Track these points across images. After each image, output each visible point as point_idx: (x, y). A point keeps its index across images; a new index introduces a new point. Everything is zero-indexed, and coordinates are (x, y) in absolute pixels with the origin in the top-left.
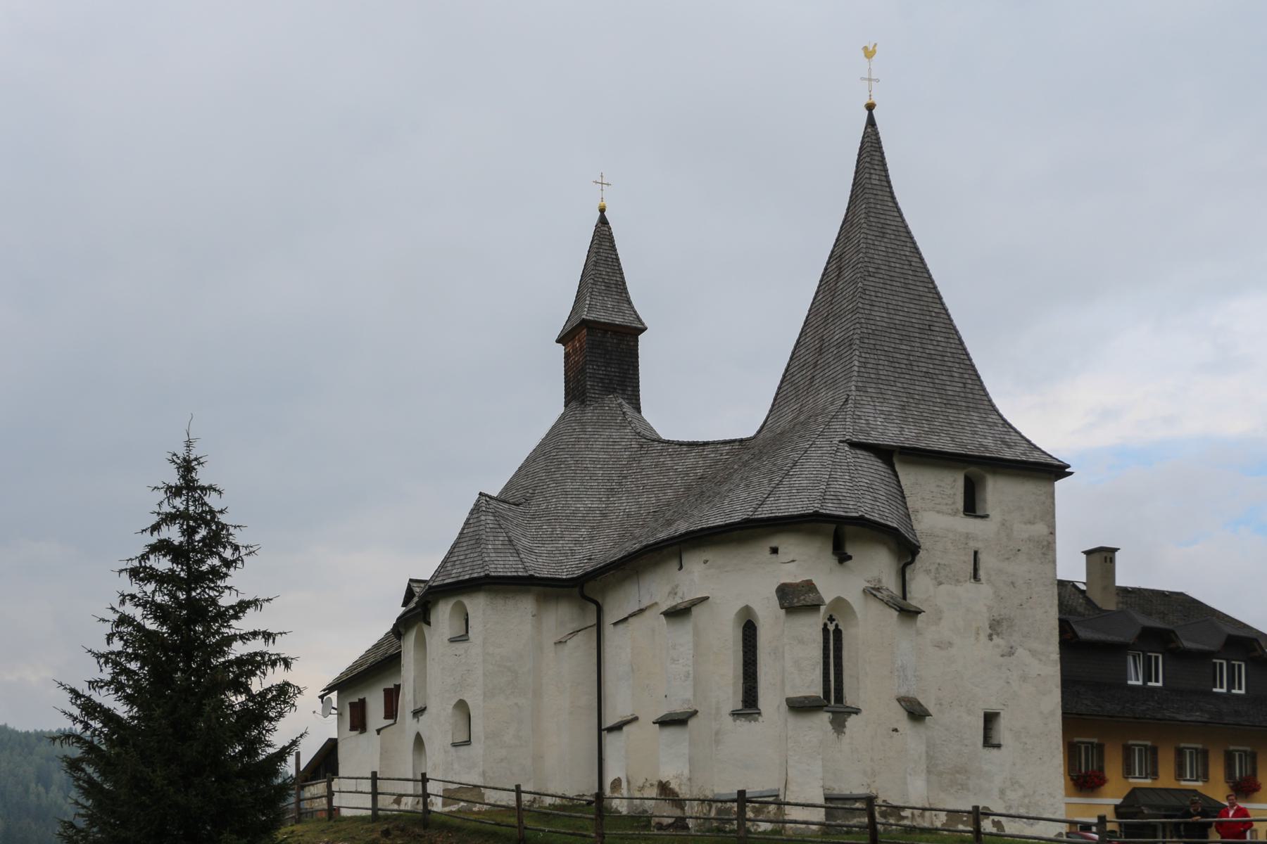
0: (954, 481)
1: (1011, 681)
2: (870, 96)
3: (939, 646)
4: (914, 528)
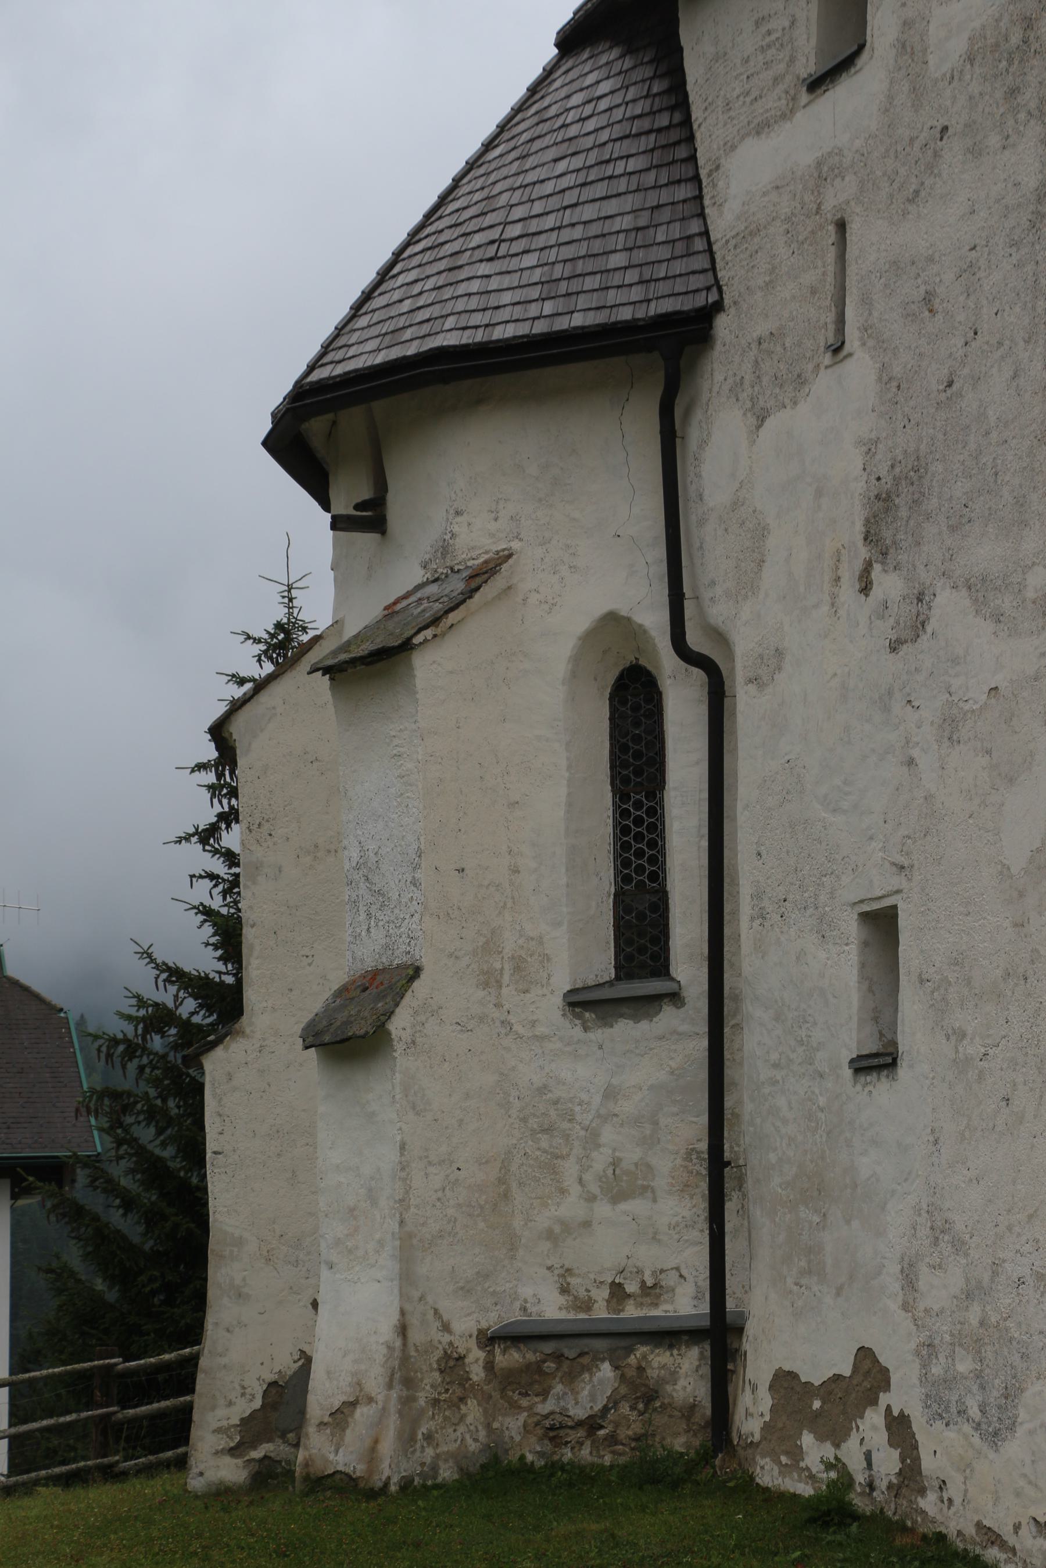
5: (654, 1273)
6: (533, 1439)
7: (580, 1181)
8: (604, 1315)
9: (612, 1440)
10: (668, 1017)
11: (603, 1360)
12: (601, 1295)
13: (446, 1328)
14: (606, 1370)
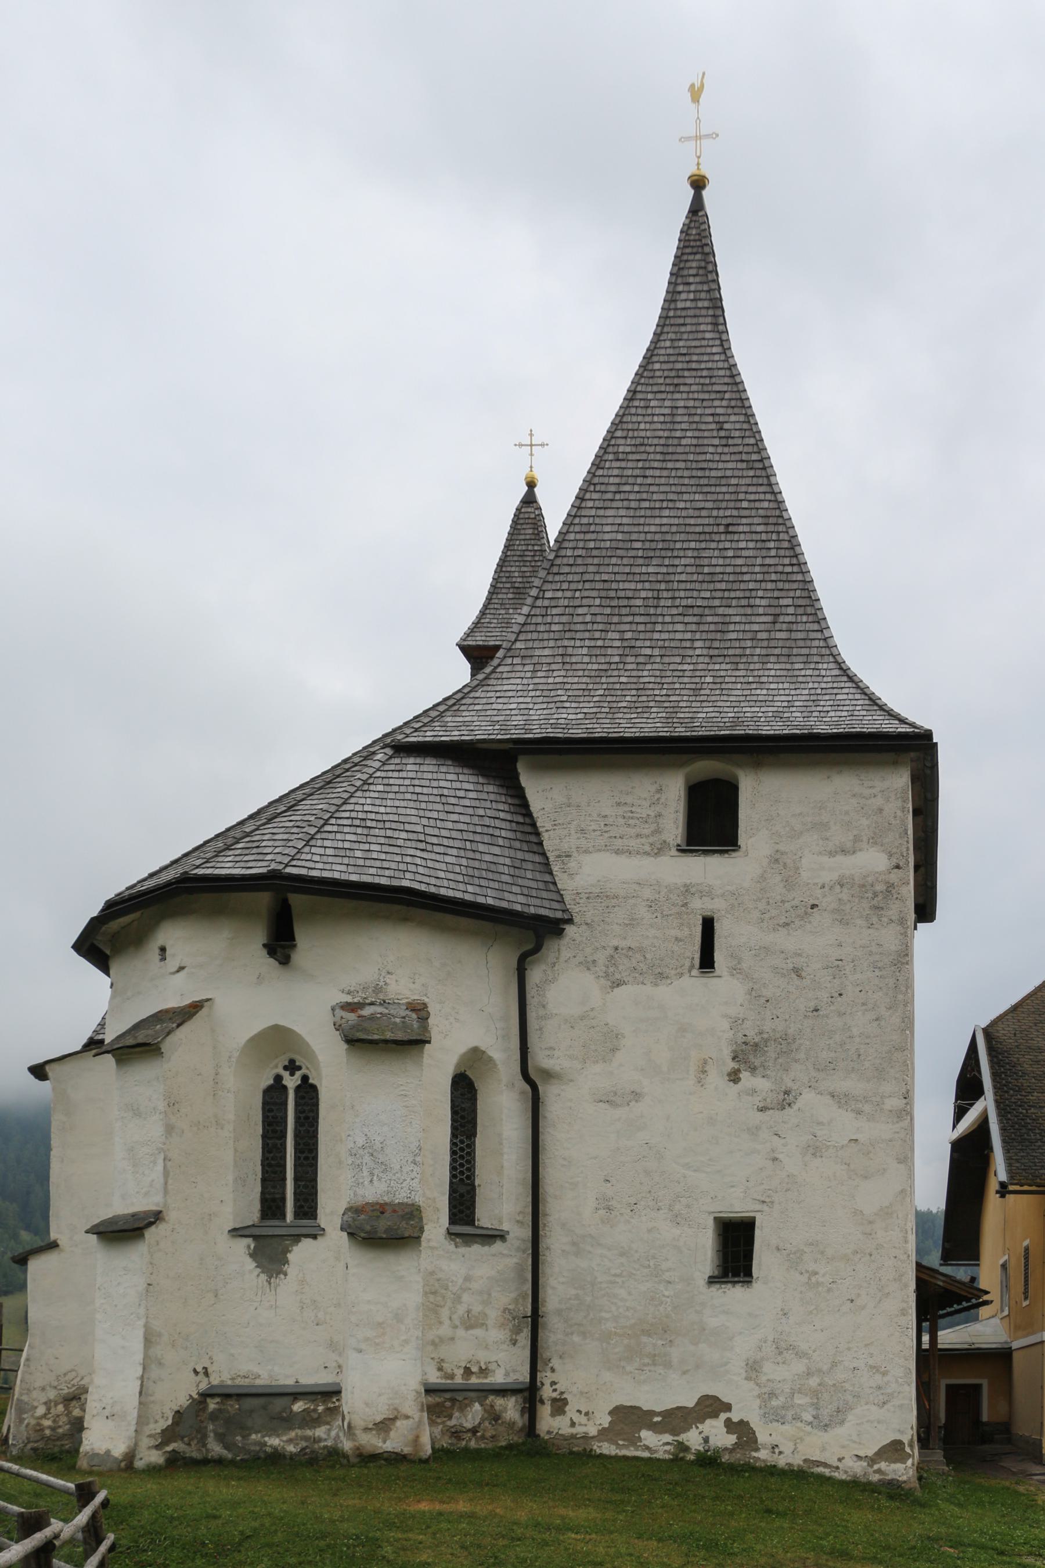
0: (660, 791)
1: (780, 1156)
2: (698, 164)
3: (609, 1100)
4: (559, 886)
5: (485, 1363)
6: (446, 1438)
7: (450, 1318)
8: (461, 1381)
9: (483, 1437)
10: (498, 1246)
11: (475, 1402)
12: (459, 1372)
14: (477, 1406)
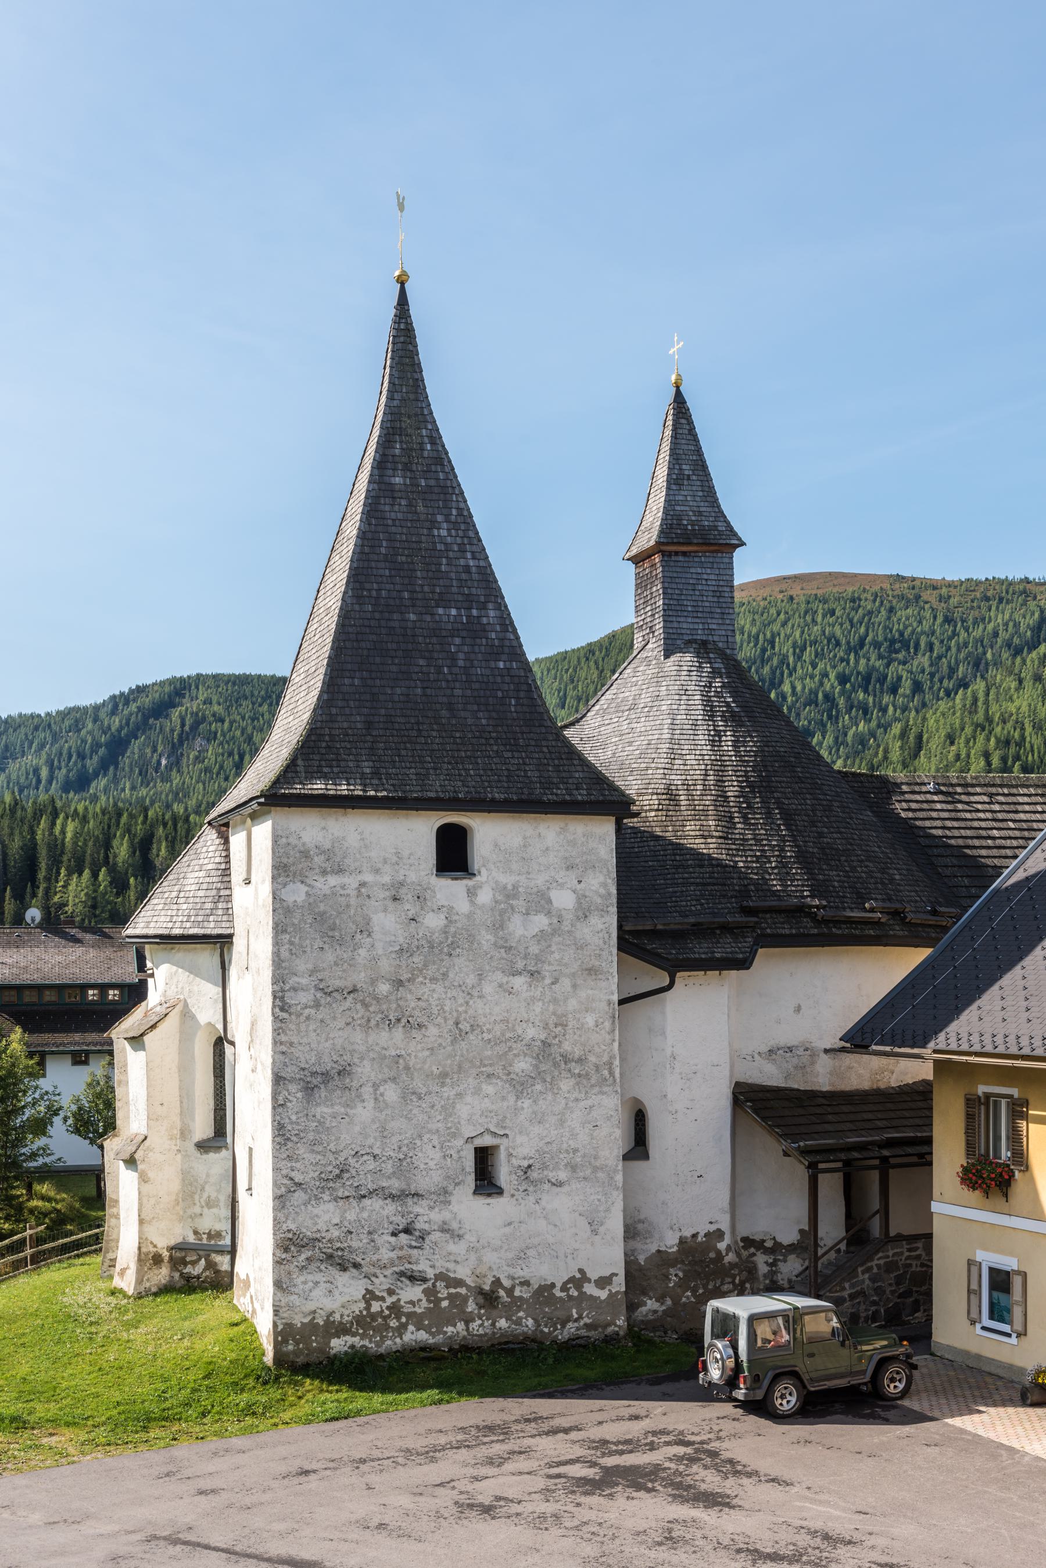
12: (205, 1236)
13: (155, 1246)
